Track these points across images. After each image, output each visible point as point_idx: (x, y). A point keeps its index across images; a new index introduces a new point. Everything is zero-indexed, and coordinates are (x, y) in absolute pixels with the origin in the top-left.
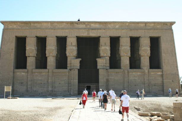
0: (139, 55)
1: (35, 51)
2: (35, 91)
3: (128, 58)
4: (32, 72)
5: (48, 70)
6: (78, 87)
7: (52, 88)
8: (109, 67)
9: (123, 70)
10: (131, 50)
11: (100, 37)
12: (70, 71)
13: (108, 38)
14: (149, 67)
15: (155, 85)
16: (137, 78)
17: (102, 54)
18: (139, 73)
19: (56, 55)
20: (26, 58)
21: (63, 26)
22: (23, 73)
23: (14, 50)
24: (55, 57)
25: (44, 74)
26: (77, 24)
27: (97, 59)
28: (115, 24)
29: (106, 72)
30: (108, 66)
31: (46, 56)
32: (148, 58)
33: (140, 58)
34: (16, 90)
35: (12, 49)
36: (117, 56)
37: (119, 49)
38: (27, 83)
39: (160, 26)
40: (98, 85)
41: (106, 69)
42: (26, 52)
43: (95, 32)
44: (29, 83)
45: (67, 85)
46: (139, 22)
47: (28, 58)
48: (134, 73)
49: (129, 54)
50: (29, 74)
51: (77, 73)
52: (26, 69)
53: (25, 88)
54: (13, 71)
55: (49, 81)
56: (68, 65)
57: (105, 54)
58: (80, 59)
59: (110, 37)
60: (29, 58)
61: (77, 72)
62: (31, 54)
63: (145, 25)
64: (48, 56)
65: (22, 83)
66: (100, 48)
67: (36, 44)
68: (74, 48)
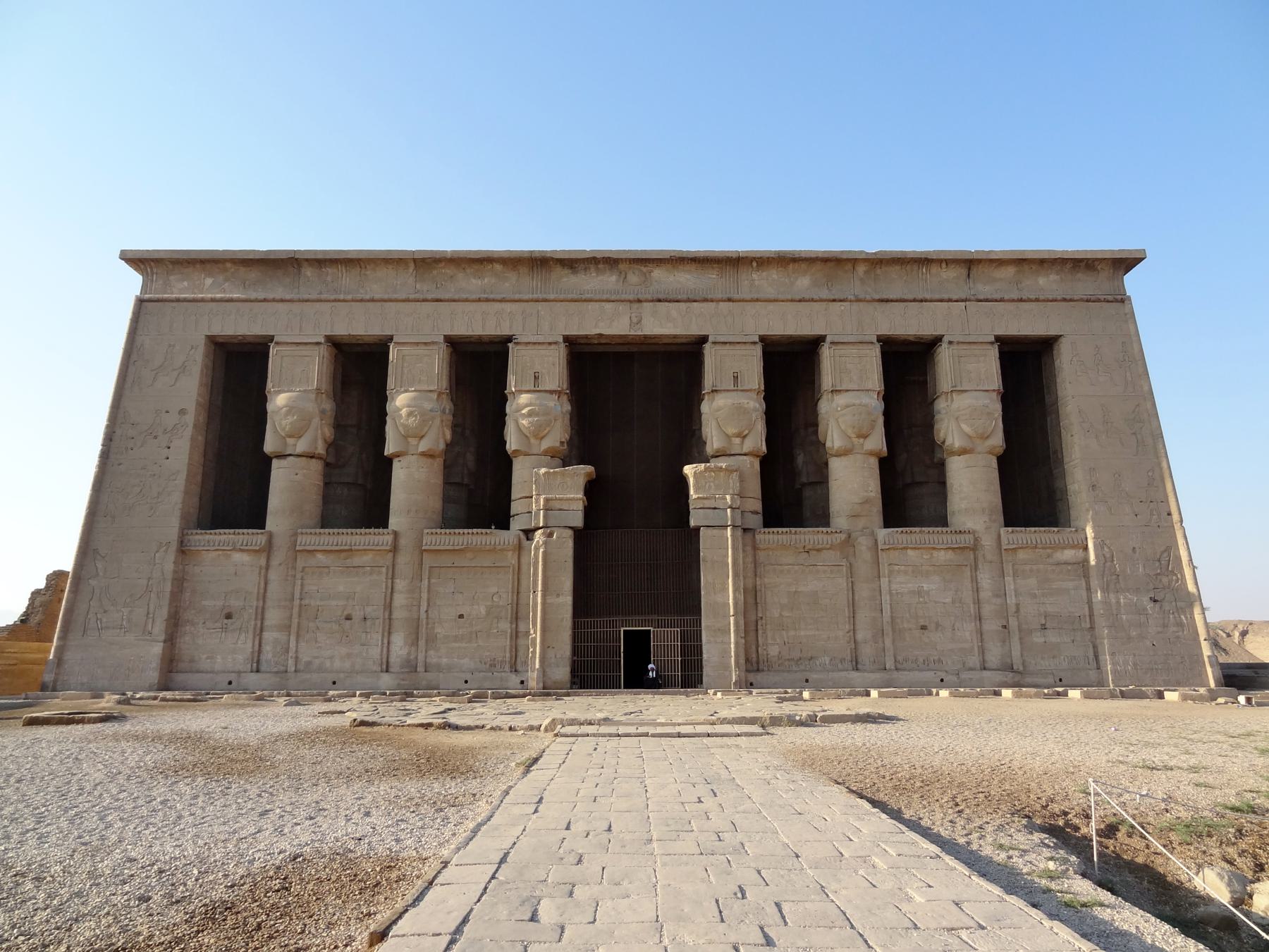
1: (316, 421)
2: (309, 663)
3: (874, 462)
4: (295, 552)
6: (576, 638)
7: (415, 642)
8: (759, 519)
9: (843, 536)
10: (886, 413)
11: (703, 340)
12: (525, 543)
13: (753, 347)
14: (1002, 519)
15: (1044, 627)
16: (933, 587)
17: (713, 437)
18: (942, 556)
19: (442, 446)
20: (265, 463)
21: (486, 280)
22: (238, 557)
23: (190, 419)
24: (438, 464)
25: (367, 559)
26: (566, 271)
27: (688, 470)
28: (791, 266)
29: (744, 545)
30: (756, 513)
31: (386, 454)
34: (192, 661)
35: (182, 412)
36: (800, 460)
37: (815, 413)
38: (261, 614)
39: (1053, 277)
40: (698, 623)
41: (745, 530)
43: (674, 313)
44: (274, 616)
45: (505, 626)
47: (275, 463)
48: (910, 552)
49: (877, 442)
50: (275, 562)
52: (262, 526)
53: (245, 644)
54: (181, 542)
55: (399, 600)
56: (515, 507)
57: (737, 441)
58: (590, 469)
59: (763, 339)
60: (283, 463)
61: (570, 544)
62: (290, 441)
63: (964, 271)
65: (229, 616)
66: (705, 407)
67: (324, 387)
68: (551, 404)
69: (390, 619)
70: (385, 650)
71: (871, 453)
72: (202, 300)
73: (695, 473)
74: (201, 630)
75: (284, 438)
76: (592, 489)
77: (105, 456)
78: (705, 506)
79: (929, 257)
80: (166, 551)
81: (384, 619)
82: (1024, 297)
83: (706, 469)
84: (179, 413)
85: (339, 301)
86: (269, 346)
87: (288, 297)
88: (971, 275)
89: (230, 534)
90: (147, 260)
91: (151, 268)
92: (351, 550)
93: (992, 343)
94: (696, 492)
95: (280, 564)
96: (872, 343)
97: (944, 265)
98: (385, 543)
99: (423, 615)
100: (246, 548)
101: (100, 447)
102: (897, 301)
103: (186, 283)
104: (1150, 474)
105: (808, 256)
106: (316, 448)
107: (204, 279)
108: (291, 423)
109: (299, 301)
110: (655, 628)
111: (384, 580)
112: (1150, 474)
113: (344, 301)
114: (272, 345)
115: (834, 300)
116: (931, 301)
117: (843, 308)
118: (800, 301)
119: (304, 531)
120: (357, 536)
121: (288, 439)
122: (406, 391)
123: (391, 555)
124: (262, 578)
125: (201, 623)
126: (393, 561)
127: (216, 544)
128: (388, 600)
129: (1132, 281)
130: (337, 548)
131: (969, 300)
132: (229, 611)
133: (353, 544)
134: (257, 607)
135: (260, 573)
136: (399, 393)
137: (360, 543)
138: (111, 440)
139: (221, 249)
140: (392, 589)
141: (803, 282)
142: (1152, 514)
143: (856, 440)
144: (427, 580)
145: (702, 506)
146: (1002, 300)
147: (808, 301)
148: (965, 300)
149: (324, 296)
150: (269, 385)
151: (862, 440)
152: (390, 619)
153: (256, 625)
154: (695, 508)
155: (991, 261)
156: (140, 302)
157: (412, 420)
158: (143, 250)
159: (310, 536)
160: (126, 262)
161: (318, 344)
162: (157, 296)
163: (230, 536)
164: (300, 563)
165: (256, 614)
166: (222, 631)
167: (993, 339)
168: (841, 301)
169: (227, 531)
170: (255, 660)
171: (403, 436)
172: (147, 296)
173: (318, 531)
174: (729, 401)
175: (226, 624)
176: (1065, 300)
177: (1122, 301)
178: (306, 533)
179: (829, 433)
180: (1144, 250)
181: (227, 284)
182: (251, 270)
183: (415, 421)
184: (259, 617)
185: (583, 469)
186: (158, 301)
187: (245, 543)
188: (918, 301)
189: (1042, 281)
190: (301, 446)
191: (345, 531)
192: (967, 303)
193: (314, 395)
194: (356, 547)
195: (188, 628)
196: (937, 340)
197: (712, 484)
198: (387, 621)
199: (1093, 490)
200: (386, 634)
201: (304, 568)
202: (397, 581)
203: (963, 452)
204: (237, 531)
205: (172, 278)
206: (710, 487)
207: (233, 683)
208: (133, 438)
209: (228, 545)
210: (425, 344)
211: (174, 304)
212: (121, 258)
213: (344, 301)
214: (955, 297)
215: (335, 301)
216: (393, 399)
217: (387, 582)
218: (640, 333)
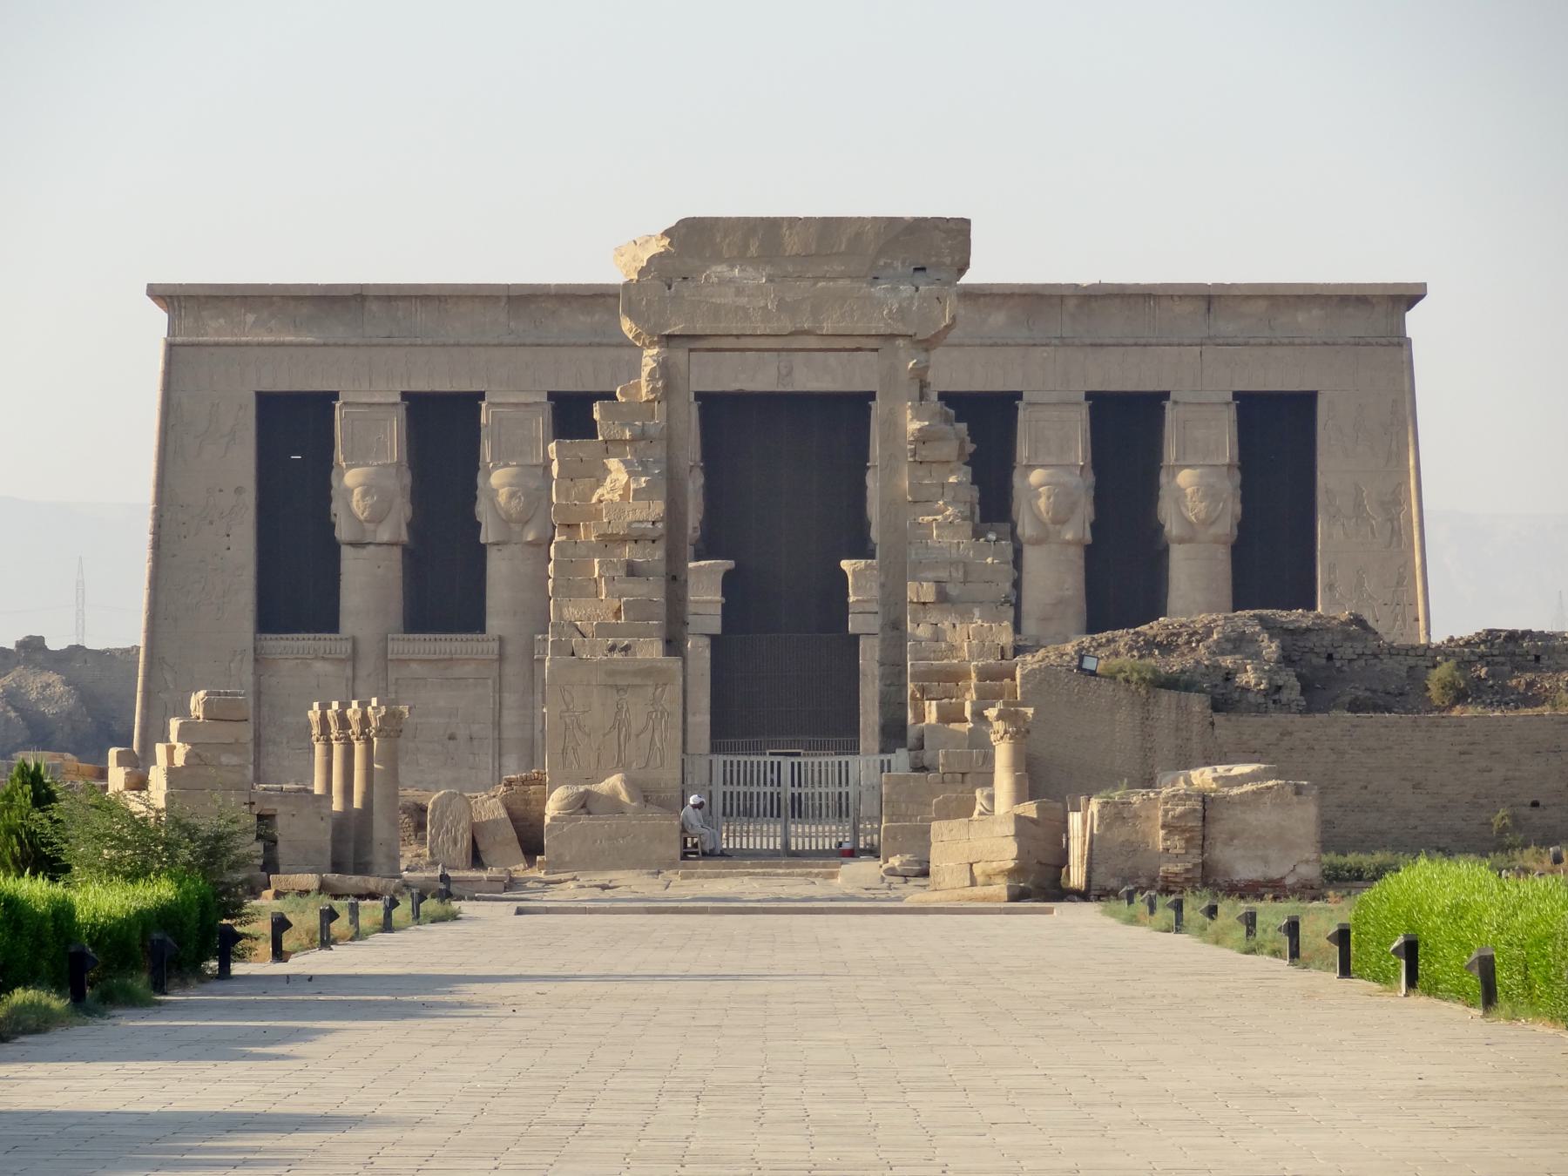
0: (1159, 528)
5: (501, 639)
21: (597, 317)
22: (319, 666)
27: (846, 565)
28: (982, 299)
31: (482, 540)
32: (1223, 555)
33: (1166, 550)
35: (239, 490)
39: (1316, 312)
42: (336, 507)
46: (1154, 285)
47: (346, 552)
49: (1077, 530)
50: (362, 672)
51: (708, 666)
55: (509, 718)
60: (364, 552)
61: (707, 654)
63: (1203, 305)
64: (497, 544)
67: (405, 458)
69: (499, 739)
70: (497, 773)
71: (1068, 543)
72: (247, 344)
73: (854, 570)
75: (360, 521)
76: (730, 583)
77: (157, 545)
78: (867, 610)
79: (1154, 293)
80: (242, 660)
81: (493, 739)
82: (1274, 341)
83: (867, 566)
84: (235, 491)
85: (416, 345)
86: (333, 408)
87: (354, 341)
88: (1212, 310)
90: (178, 297)
91: (179, 302)
92: (451, 659)
93: (1228, 404)
94: (857, 590)
95: (369, 675)
96: (1077, 404)
97: (1176, 299)
98: (490, 651)
99: (538, 735)
100: (330, 656)
101: (150, 537)
102: (1114, 345)
103: (222, 321)
104: (1401, 570)
105: (1000, 292)
106: (400, 535)
107: (245, 315)
108: (371, 506)
109: (367, 345)
110: (806, 750)
111: (491, 694)
112: (1401, 570)
113: (421, 345)
114: (338, 405)
115: (1035, 345)
116: (1158, 345)
117: (1045, 355)
118: (991, 346)
119: (395, 636)
120: (456, 643)
121: (365, 524)
122: (506, 465)
123: (496, 665)
126: (500, 672)
127: (295, 652)
128: (497, 718)
129: (1415, 321)
130: (435, 657)
131: (1205, 345)
133: (453, 651)
135: (347, 685)
136: (495, 467)
137: (461, 652)
138: (160, 526)
139: (270, 283)
140: (500, 703)
141: (998, 319)
142: (1395, 620)
143: (1051, 527)
144: (540, 695)
145: (861, 610)
146: (1246, 344)
147: (1003, 345)
148: (1201, 345)
149: (395, 341)
150: (339, 455)
151: (1058, 527)
152: (499, 739)
154: (853, 613)
155: (1235, 296)
156: (171, 348)
157: (514, 502)
158: (175, 284)
159: (401, 643)
160: (153, 300)
161: (394, 404)
162: (190, 339)
164: (392, 676)
167: (1230, 397)
168: (1043, 345)
169: (306, 636)
171: (503, 520)
172: (179, 339)
173: (400, 636)
174: (906, 469)
176: (1326, 344)
177: (1400, 345)
178: (398, 640)
179: (1021, 517)
180: (1425, 284)
181: (273, 322)
182: (302, 304)
183: (519, 503)
185: (721, 565)
186: (193, 345)
187: (328, 651)
188: (1140, 345)
189: (1301, 318)
190: (384, 535)
191: (443, 636)
192: (1204, 347)
193: (395, 471)
194: (458, 656)
196: (1165, 395)
197: (873, 584)
198: (497, 741)
199: (1330, 589)
200: (497, 756)
201: (397, 679)
202: (506, 695)
203: (1181, 541)
204: (318, 635)
205: (204, 313)
206: (871, 588)
208: (184, 523)
210: (527, 405)
211: (212, 350)
212: (149, 296)
213: (421, 345)
214: (1187, 341)
215: (411, 345)
216: (489, 474)
217: (494, 697)
218: (789, 389)
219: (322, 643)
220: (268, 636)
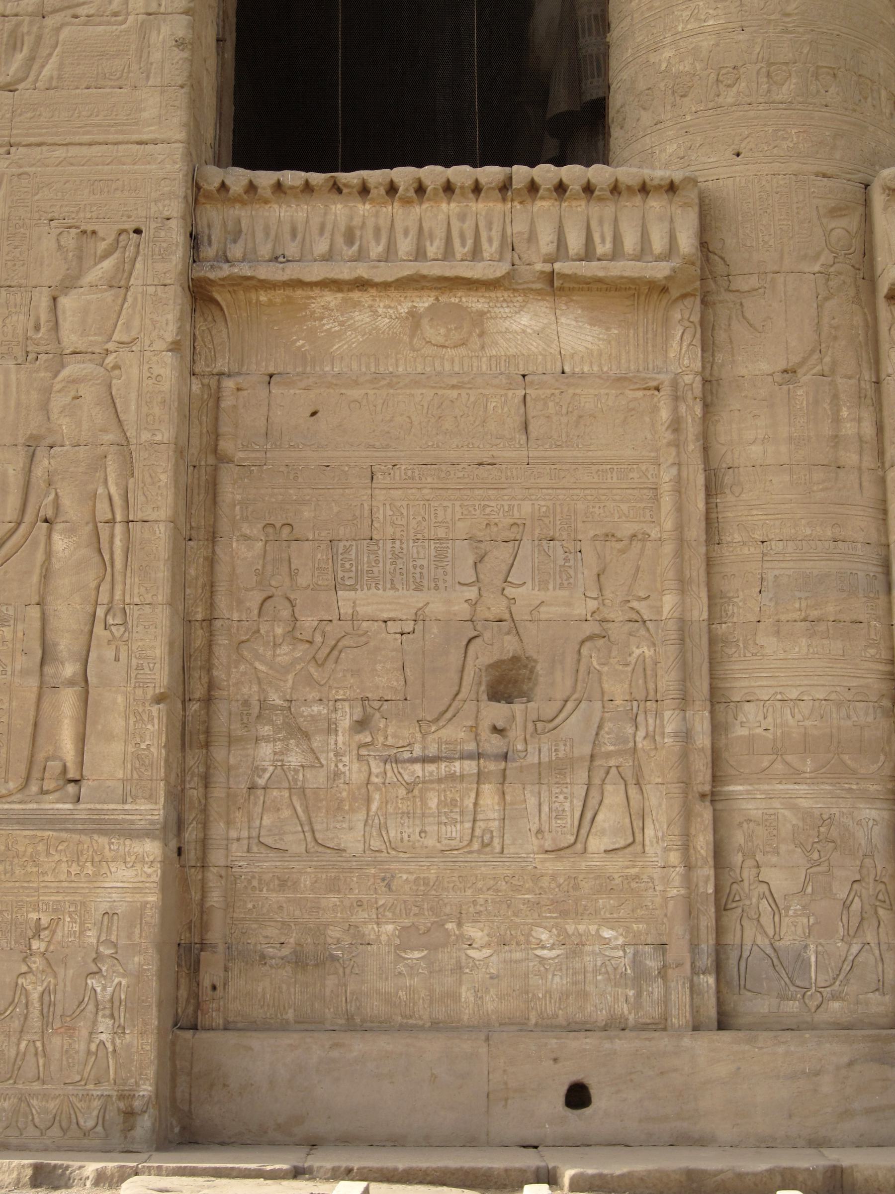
54: (195, 240)
74: (353, 771)
89: (477, 189)
95: (790, 372)
124: (693, 447)
125: (345, 723)
132: (509, 646)
134: (683, 625)
135: (676, 425)
153: (686, 736)
163: (479, 207)
165: (685, 679)
166: (480, 777)
170: (706, 960)
175: (496, 730)
184: (701, 686)
195: (266, 751)
207: (600, 1100)
209: (476, 254)
219: (543, 205)
220: (265, 178)
